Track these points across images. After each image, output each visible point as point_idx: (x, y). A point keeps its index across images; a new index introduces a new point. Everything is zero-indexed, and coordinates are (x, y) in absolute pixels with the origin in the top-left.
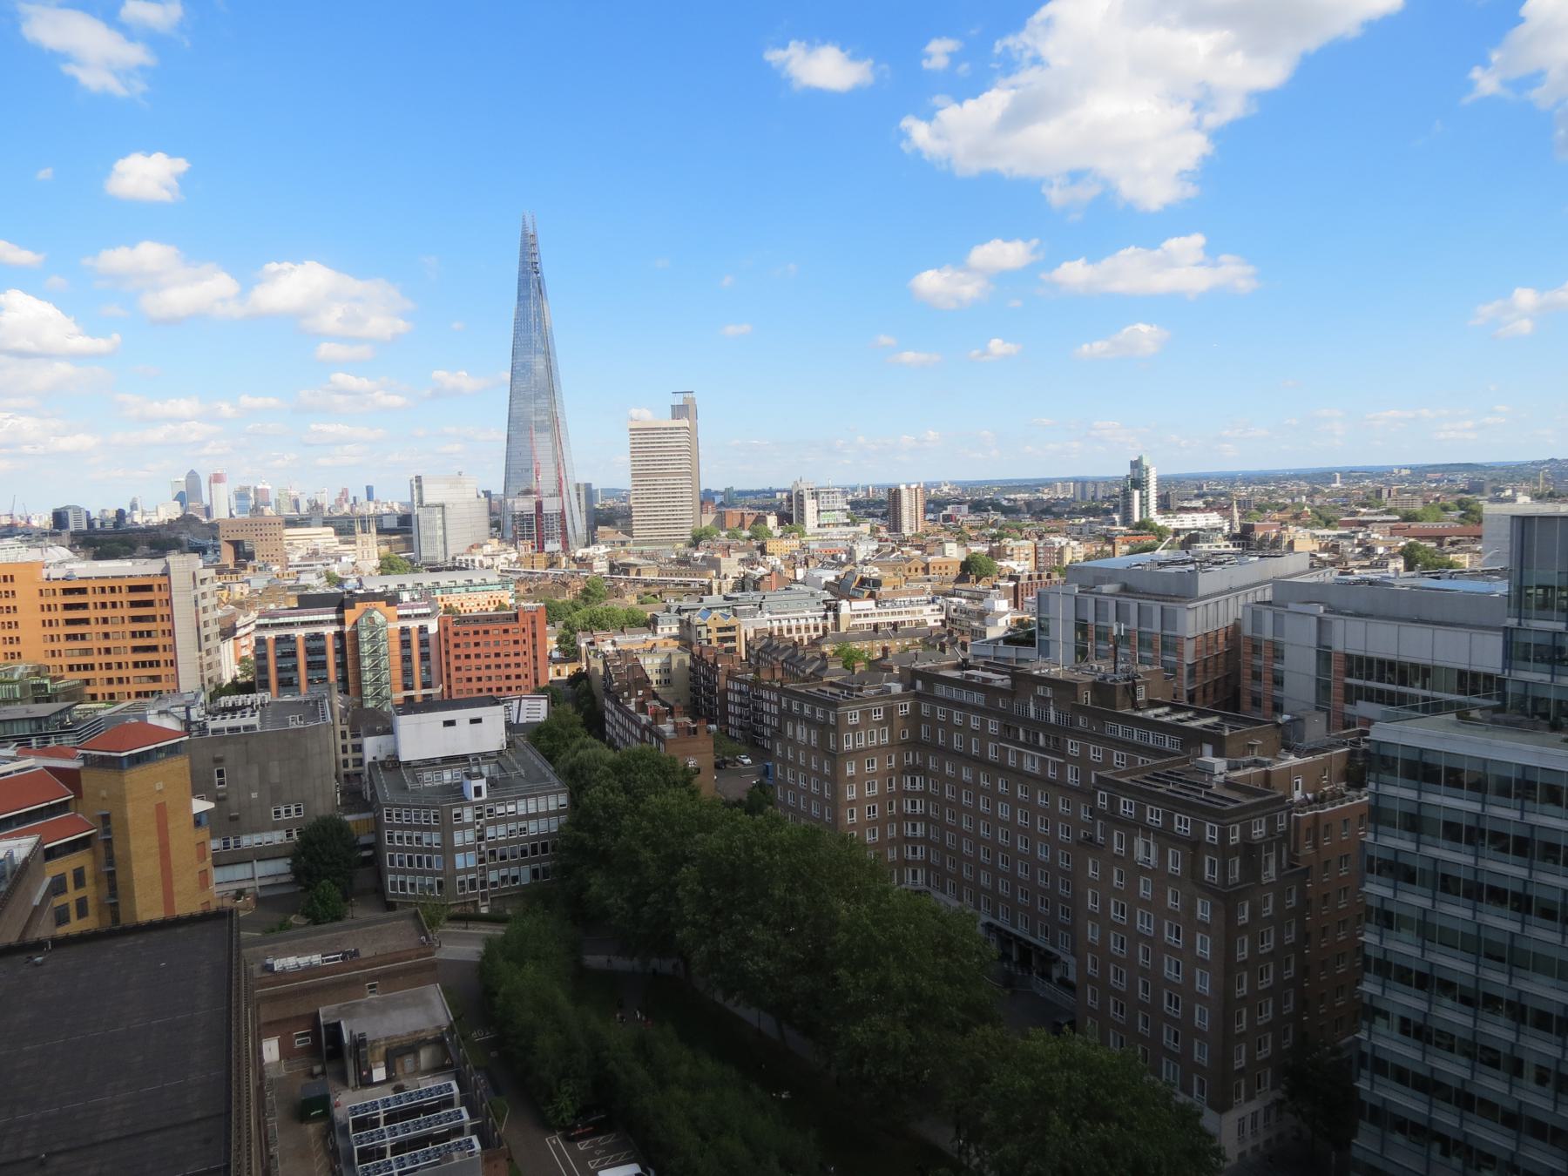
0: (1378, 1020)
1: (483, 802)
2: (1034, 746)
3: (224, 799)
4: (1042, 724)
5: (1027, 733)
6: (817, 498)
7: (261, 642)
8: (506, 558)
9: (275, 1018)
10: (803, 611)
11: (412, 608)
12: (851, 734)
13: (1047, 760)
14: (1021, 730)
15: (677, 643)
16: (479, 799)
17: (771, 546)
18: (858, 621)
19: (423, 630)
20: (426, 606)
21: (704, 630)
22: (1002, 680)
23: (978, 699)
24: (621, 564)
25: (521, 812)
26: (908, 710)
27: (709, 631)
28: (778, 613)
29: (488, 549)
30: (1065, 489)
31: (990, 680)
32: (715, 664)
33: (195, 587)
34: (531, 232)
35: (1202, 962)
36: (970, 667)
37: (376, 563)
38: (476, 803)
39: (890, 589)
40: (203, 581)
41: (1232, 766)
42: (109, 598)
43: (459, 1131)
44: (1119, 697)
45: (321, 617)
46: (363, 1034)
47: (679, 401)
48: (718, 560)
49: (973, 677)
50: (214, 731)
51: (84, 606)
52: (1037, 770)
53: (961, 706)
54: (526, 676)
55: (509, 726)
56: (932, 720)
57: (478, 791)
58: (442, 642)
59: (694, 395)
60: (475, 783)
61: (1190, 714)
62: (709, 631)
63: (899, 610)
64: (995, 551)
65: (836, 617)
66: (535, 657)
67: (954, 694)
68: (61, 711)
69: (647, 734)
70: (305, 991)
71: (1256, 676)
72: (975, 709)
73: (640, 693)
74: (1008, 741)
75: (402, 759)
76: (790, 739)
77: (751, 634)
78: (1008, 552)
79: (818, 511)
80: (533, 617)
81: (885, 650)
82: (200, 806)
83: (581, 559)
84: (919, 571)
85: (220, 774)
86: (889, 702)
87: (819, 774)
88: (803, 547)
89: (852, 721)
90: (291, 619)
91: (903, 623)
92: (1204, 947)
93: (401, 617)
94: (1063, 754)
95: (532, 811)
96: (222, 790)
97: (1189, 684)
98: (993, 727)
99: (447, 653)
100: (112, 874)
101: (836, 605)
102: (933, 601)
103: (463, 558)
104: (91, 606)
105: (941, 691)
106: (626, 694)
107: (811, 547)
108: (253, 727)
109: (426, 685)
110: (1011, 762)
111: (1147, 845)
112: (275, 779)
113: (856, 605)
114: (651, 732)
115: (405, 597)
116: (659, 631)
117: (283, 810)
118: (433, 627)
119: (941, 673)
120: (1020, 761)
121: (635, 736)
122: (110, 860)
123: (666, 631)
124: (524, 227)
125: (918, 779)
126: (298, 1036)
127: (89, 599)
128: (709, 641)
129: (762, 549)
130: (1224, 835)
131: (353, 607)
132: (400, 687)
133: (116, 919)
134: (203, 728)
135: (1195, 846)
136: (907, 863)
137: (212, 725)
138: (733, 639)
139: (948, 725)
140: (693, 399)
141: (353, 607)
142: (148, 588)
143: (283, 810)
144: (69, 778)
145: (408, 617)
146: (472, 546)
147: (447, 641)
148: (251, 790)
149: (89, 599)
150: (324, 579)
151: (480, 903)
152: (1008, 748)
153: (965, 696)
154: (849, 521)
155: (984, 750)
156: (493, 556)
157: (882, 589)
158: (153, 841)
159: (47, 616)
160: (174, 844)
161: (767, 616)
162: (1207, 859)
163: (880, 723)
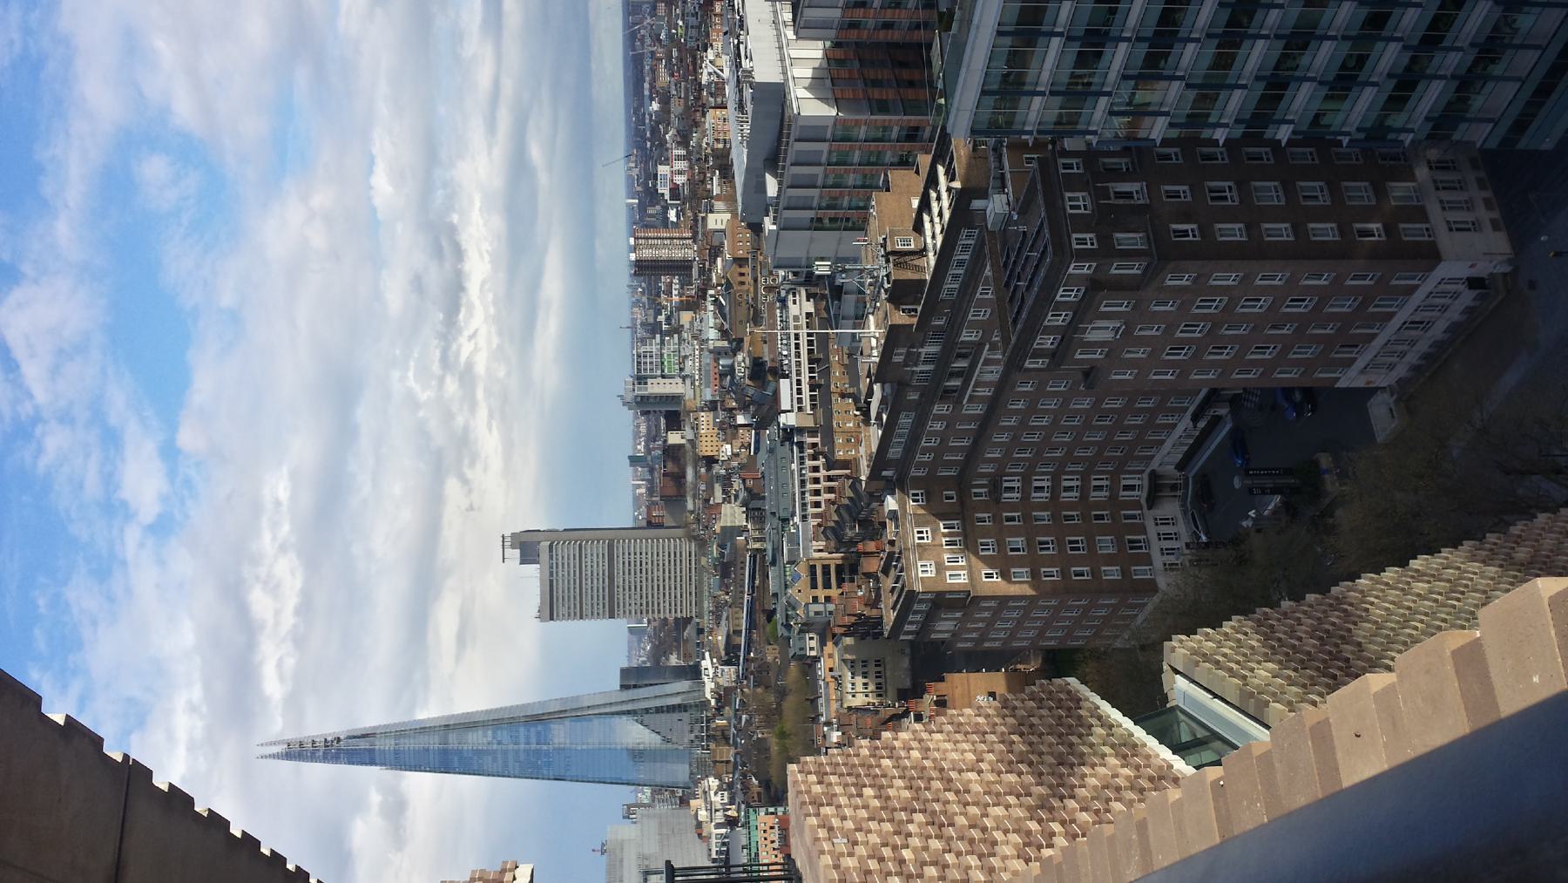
0: (1325, 121)
2: (966, 375)
4: (942, 361)
10: (792, 472)
12: (948, 573)
13: (986, 360)
15: (830, 644)
17: (706, 448)
18: (807, 403)
21: (814, 608)
24: (726, 654)
26: (919, 492)
28: (794, 506)
29: (703, 815)
30: (639, 486)
32: (861, 615)
35: (1246, 280)
39: (766, 347)
41: (999, 183)
44: (909, 275)
52: (1000, 368)
56: (933, 466)
59: (508, 534)
61: (933, 195)
62: (815, 599)
63: (793, 346)
64: (719, 162)
65: (800, 430)
71: (888, 26)
76: (953, 635)
77: (821, 544)
78: (721, 146)
81: (843, 396)
83: (718, 700)
84: (743, 270)
87: (996, 613)
88: (712, 406)
89: (931, 573)
91: (810, 352)
92: (1225, 278)
94: (979, 346)
97: (896, 113)
98: (939, 409)
101: (785, 430)
102: (783, 301)
103: (714, 849)
105: (895, 452)
107: (709, 398)
111: (1092, 329)
113: (785, 403)
116: (813, 653)
119: (874, 449)
120: (986, 384)
123: (813, 644)
125: (1006, 485)
128: (828, 599)
129: (711, 461)
130: (1083, 255)
135: (1096, 286)
136: (1113, 497)
138: (826, 569)
140: (514, 535)
146: (700, 835)
152: (970, 395)
154: (676, 336)
155: (971, 418)
156: (711, 810)
157: (766, 358)
161: (797, 519)
162: (1113, 271)
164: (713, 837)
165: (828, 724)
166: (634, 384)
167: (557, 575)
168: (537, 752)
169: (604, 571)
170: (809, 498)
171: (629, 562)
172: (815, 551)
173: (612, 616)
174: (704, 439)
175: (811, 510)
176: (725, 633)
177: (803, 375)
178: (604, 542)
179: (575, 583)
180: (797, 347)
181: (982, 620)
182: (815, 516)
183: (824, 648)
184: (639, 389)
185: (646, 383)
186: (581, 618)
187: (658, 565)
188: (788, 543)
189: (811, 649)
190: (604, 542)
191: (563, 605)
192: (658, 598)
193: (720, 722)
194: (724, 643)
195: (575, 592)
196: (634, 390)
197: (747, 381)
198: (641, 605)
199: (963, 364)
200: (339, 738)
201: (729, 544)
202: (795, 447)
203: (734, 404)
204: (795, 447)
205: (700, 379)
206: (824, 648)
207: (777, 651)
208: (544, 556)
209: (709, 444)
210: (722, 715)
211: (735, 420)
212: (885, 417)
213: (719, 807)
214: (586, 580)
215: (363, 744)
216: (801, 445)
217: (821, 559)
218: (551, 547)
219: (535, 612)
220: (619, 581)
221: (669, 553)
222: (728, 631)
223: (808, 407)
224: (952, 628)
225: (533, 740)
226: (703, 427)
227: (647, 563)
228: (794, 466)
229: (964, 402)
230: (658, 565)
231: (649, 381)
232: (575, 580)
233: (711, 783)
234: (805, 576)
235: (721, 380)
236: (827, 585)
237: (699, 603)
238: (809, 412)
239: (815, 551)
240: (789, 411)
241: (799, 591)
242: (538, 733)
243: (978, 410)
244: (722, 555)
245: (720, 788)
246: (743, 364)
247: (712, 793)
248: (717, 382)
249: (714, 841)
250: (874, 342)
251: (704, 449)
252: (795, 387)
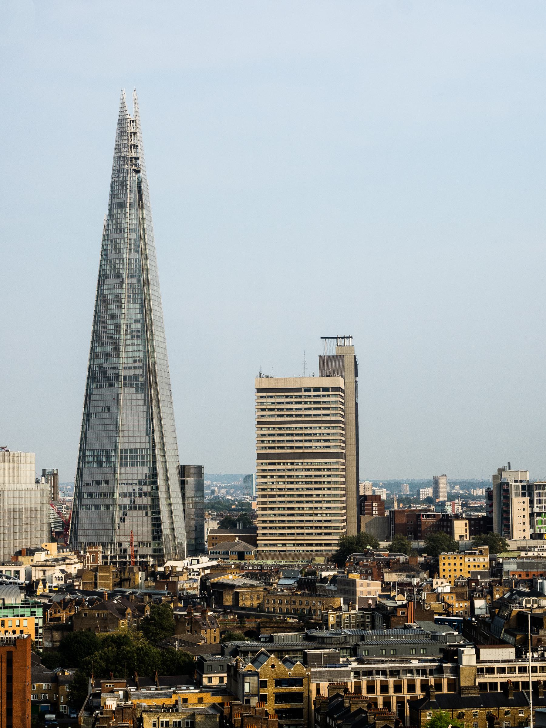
6: (530, 495)
8: (63, 571)
10: (408, 661)
18: (488, 679)
24: (213, 584)
27: (263, 684)
28: (369, 662)
29: (40, 557)
34: (130, 116)
47: (330, 349)
48: (354, 582)
65: (456, 670)
77: (325, 692)
79: (532, 515)
80: (10, 654)
83: (162, 574)
107: (506, 567)
113: (487, 654)
116: (205, 681)
123: (216, 682)
124: (123, 111)
128: (263, 699)
146: (19, 553)
156: (44, 566)
161: (354, 665)
164: (17, 568)
165: (127, 696)
166: (521, 481)
167: (306, 396)
168: (115, 378)
169: (310, 447)
170: (378, 680)
171: (320, 476)
172: (318, 685)
173: (260, 456)
174: (458, 561)
175: (364, 681)
176: (237, 583)
177: (520, 675)
178: (343, 448)
179: (297, 416)
182: (358, 688)
183: (209, 694)
184: (517, 487)
185: (524, 495)
186: (259, 423)
187: (316, 508)
188: (328, 654)
189: (210, 680)
190: (343, 448)
191: (273, 403)
192: (279, 508)
193: (140, 576)
194: (225, 581)
195: (287, 416)
196: (516, 481)
197: (515, 611)
198: (272, 489)
200: (139, 171)
201: (335, 588)
202: (437, 664)
203: (498, 596)
204: (437, 664)
205: (528, 558)
206: (209, 694)
207: (212, 641)
208: (327, 382)
209: (452, 567)
210: (146, 580)
211: (479, 598)
213: (48, 573)
214: (301, 428)
215: (131, 197)
216: (440, 670)
217: (309, 691)
220: (300, 464)
221: (329, 521)
222: (238, 587)
223: (482, 680)
225: (130, 373)
226: (472, 560)
227: (318, 495)
228: (415, 663)
230: (316, 508)
231: (527, 499)
232: (300, 416)
233: (74, 566)
234: (291, 671)
235: (524, 581)
236: (279, 698)
237: (272, 555)
238: (478, 681)
239: (318, 685)
240: (478, 657)
241: (273, 666)
242: (135, 378)
244: (324, 580)
245: (68, 576)
246: (535, 605)
247: (63, 567)
248: (524, 577)
249: (13, 568)
251: (446, 561)
252: (506, 665)
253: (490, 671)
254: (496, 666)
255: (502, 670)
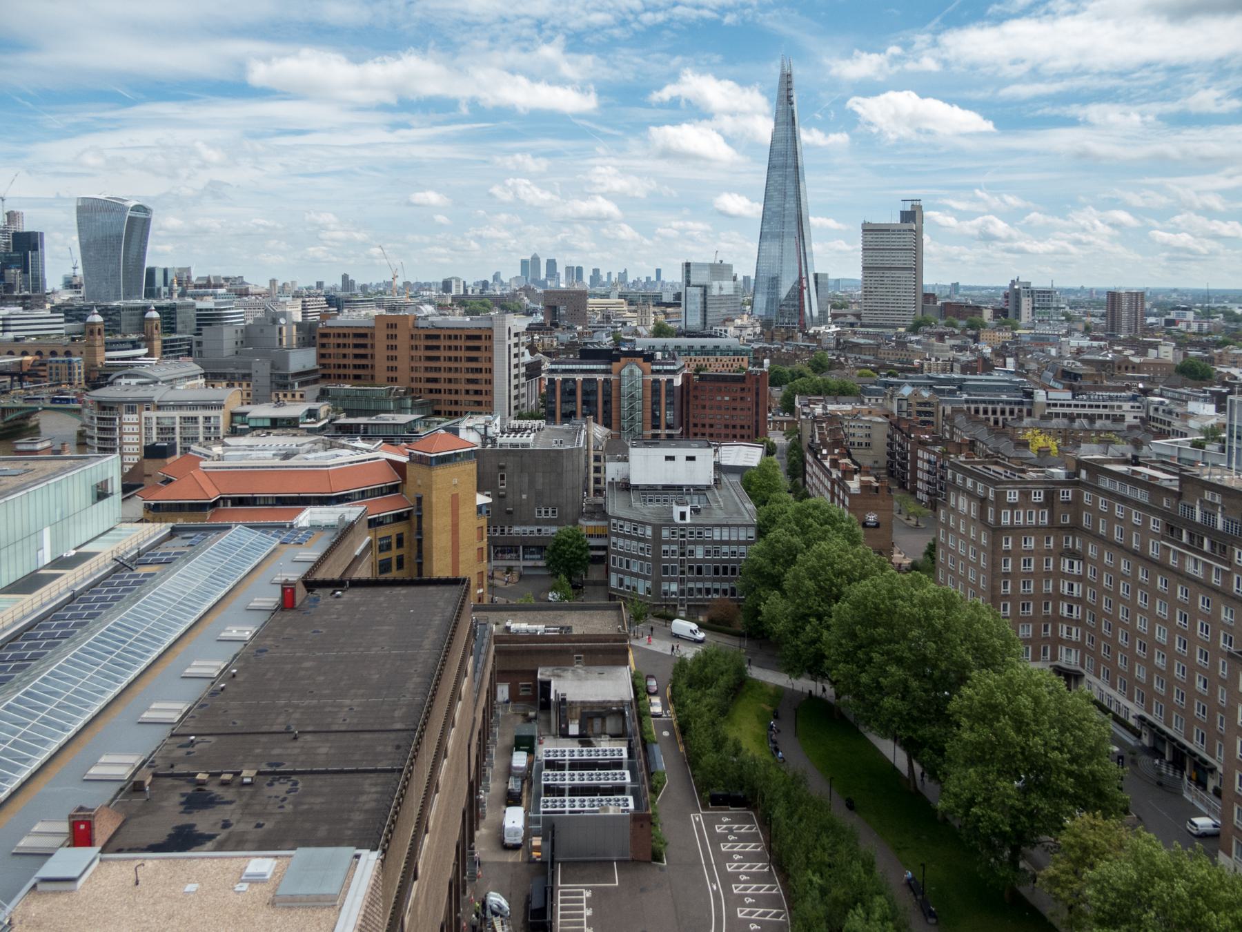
1: (686, 525)
3: (503, 497)
5: (1191, 536)
7: (552, 381)
9: (507, 668)
11: (663, 364)
14: (1184, 532)
16: (683, 522)
19: (670, 381)
20: (674, 364)
22: (1171, 480)
23: (1141, 495)
25: (717, 538)
26: (1070, 496)
29: (738, 322)
31: (1157, 479)
33: (509, 338)
36: (1138, 464)
37: (651, 327)
38: (681, 525)
40: (516, 335)
42: (454, 343)
43: (620, 790)
45: (595, 367)
46: (564, 695)
49: (1140, 473)
50: (501, 445)
51: (438, 348)
53: (1123, 499)
54: (749, 427)
55: (718, 467)
56: (1093, 509)
57: (683, 516)
58: (685, 393)
59: (922, 203)
60: (682, 509)
63: (1083, 403)
66: (757, 414)
67: (1118, 487)
68: (415, 421)
69: (836, 487)
70: (529, 652)
72: (1138, 505)
73: (836, 451)
74: (1169, 541)
75: (633, 482)
82: (482, 499)
85: (502, 477)
86: (1051, 486)
90: (574, 367)
93: (653, 372)
95: (725, 538)
96: (502, 490)
98: (1155, 524)
99: (688, 403)
100: (420, 541)
104: (442, 348)
105: (1105, 483)
106: (824, 452)
108: (528, 445)
109: (669, 427)
110: (1172, 562)
112: (539, 487)
114: (839, 486)
115: (659, 355)
117: (543, 510)
118: (678, 381)
121: (826, 488)
122: (420, 531)
126: (522, 686)
127: (443, 343)
131: (619, 361)
132: (650, 426)
133: (420, 574)
134: (494, 441)
137: (499, 440)
139: (1110, 517)
140: (920, 207)
141: (619, 361)
142: (478, 338)
143: (543, 510)
144: (398, 467)
145: (658, 372)
147: (688, 393)
148: (521, 492)
149: (443, 343)
150: (611, 338)
151: (679, 608)
153: (1128, 491)
155: (1145, 546)
158: (447, 520)
159: (414, 353)
160: (462, 525)
163: (1040, 505)
170: (982, 406)
173: (864, 268)
175: (973, 406)
180: (1098, 407)
181: (968, 531)
182: (969, 409)
199: (1206, 546)
212: (1139, 477)
218: (912, 230)
219: (868, 220)
220: (888, 274)
224: (960, 508)
228: (1004, 397)
229: (1163, 542)
236: (919, 413)
238: (1047, 411)
243: (1153, 553)
245: (755, 334)
250: (1218, 477)
252: (1066, 402)
253: (1055, 405)
254: (1059, 402)
255: (1062, 405)
